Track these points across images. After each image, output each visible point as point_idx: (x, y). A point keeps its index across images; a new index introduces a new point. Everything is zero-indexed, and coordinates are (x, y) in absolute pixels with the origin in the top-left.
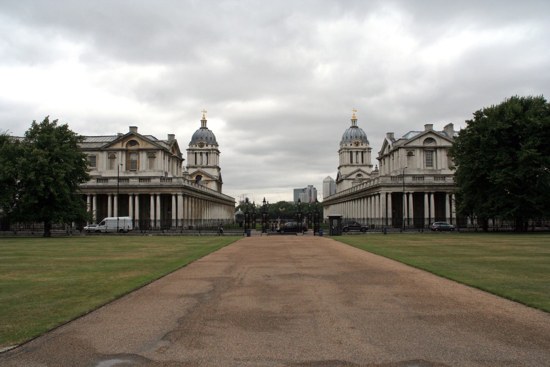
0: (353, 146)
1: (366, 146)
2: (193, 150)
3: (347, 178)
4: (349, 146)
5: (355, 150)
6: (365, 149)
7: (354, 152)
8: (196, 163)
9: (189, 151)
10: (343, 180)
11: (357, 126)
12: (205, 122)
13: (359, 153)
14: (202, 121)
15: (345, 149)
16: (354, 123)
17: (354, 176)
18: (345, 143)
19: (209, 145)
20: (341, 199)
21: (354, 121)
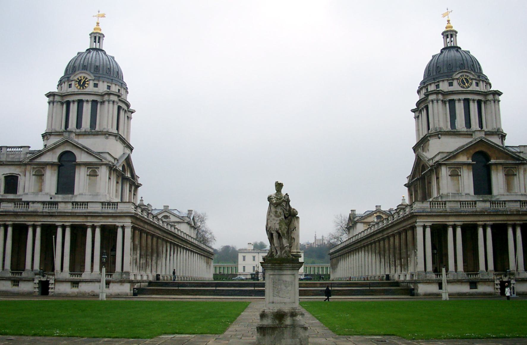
1: (486, 89)
2: (62, 96)
4: (444, 86)
5: (463, 97)
6: (486, 94)
7: (459, 100)
8: (67, 126)
11: (458, 45)
13: (471, 104)
18: (434, 83)
19: (100, 84)
21: (452, 37)
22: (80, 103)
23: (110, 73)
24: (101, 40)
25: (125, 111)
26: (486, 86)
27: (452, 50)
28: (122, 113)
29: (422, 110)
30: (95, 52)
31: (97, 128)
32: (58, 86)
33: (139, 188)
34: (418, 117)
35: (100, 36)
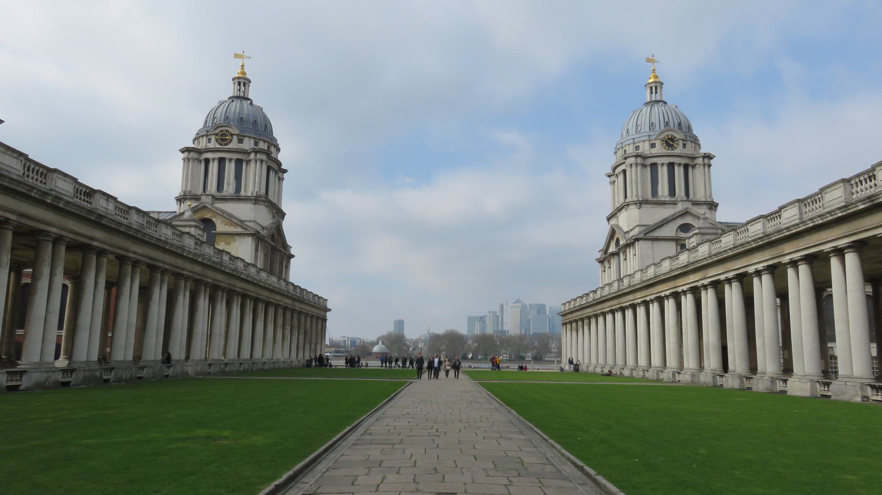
0: (659, 149)
1: (695, 151)
2: (200, 152)
3: (648, 235)
4: (645, 148)
7: (663, 164)
9: (186, 153)
10: (638, 240)
11: (663, 100)
12: (244, 85)
13: (676, 168)
14: (236, 80)
15: (636, 156)
16: (656, 92)
17: (670, 231)
19: (246, 140)
20: (692, 278)
22: (222, 161)
23: (258, 126)
24: (247, 86)
25: (276, 172)
26: (694, 147)
27: (656, 106)
28: (272, 174)
29: (619, 175)
30: (239, 101)
31: (242, 193)
32: (194, 140)
33: (292, 260)
34: (615, 181)
35: (245, 81)
